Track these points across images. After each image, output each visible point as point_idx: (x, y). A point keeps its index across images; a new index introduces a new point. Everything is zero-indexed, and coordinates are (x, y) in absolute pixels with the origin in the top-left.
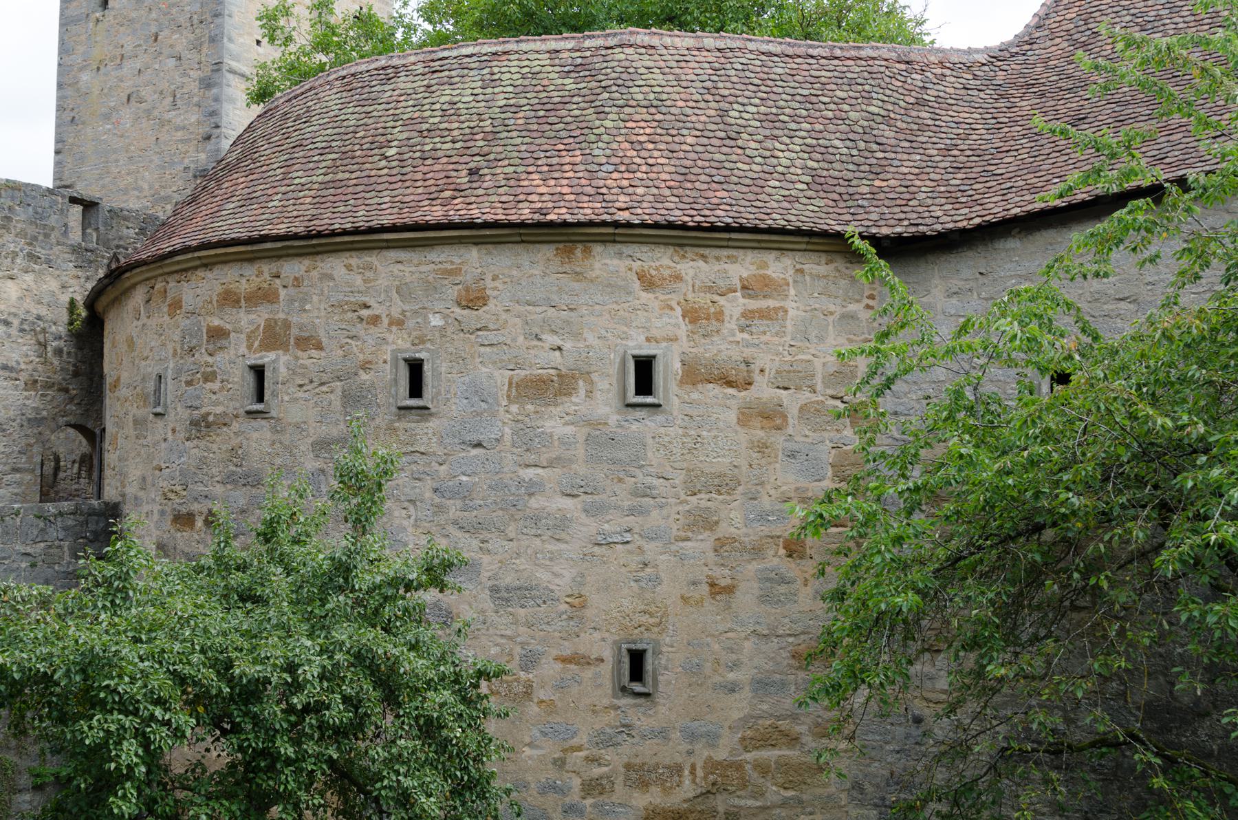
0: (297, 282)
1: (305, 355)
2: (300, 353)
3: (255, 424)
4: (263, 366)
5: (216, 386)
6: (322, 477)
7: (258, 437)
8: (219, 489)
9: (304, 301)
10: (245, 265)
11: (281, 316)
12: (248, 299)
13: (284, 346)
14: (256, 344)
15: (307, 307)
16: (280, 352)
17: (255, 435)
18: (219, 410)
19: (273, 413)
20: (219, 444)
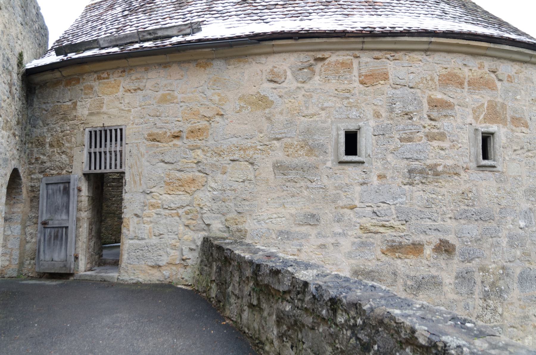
0: (510, 79)
1: (519, 130)
2: (514, 128)
3: (482, 174)
4: (493, 134)
5: (446, 144)
6: (532, 214)
7: (485, 185)
8: (451, 224)
9: (516, 93)
10: (468, 58)
11: (499, 100)
12: (469, 84)
13: (504, 121)
14: (482, 117)
15: (518, 97)
16: (501, 125)
17: (484, 183)
18: (450, 162)
19: (499, 168)
20: (447, 189)
